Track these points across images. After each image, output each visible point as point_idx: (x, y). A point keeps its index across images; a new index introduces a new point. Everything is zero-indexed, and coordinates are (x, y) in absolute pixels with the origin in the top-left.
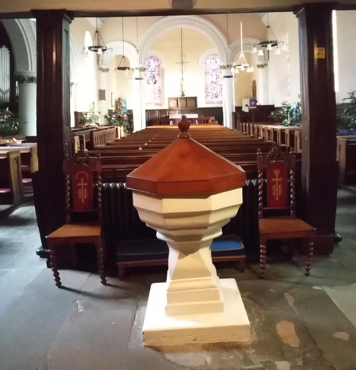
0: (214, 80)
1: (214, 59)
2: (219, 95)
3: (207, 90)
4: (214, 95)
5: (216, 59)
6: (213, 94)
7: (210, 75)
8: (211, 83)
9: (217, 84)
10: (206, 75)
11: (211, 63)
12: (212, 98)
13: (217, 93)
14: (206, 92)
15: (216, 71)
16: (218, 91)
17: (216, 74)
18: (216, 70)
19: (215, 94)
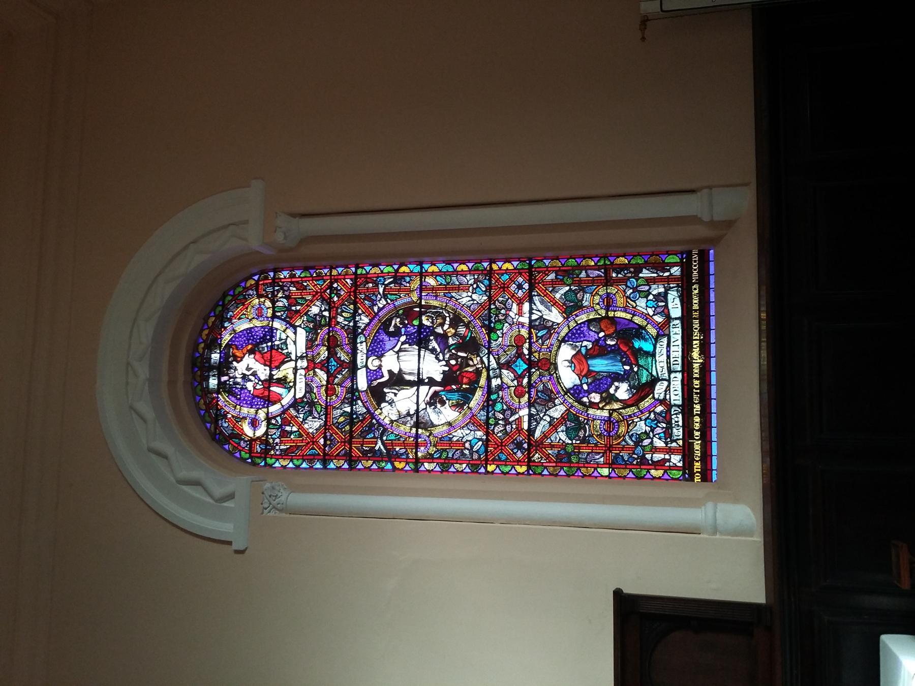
0: (434, 368)
1: (224, 367)
2: (609, 301)
3: (539, 445)
4: (600, 365)
5: (226, 338)
6: (602, 383)
7: (387, 413)
8: (467, 396)
9: (482, 335)
10: (376, 456)
11: (269, 400)
12: (643, 390)
13: (574, 336)
14: (564, 458)
15: (343, 337)
16: (554, 316)
17: (377, 351)
18: (332, 345)
19: (600, 350)
